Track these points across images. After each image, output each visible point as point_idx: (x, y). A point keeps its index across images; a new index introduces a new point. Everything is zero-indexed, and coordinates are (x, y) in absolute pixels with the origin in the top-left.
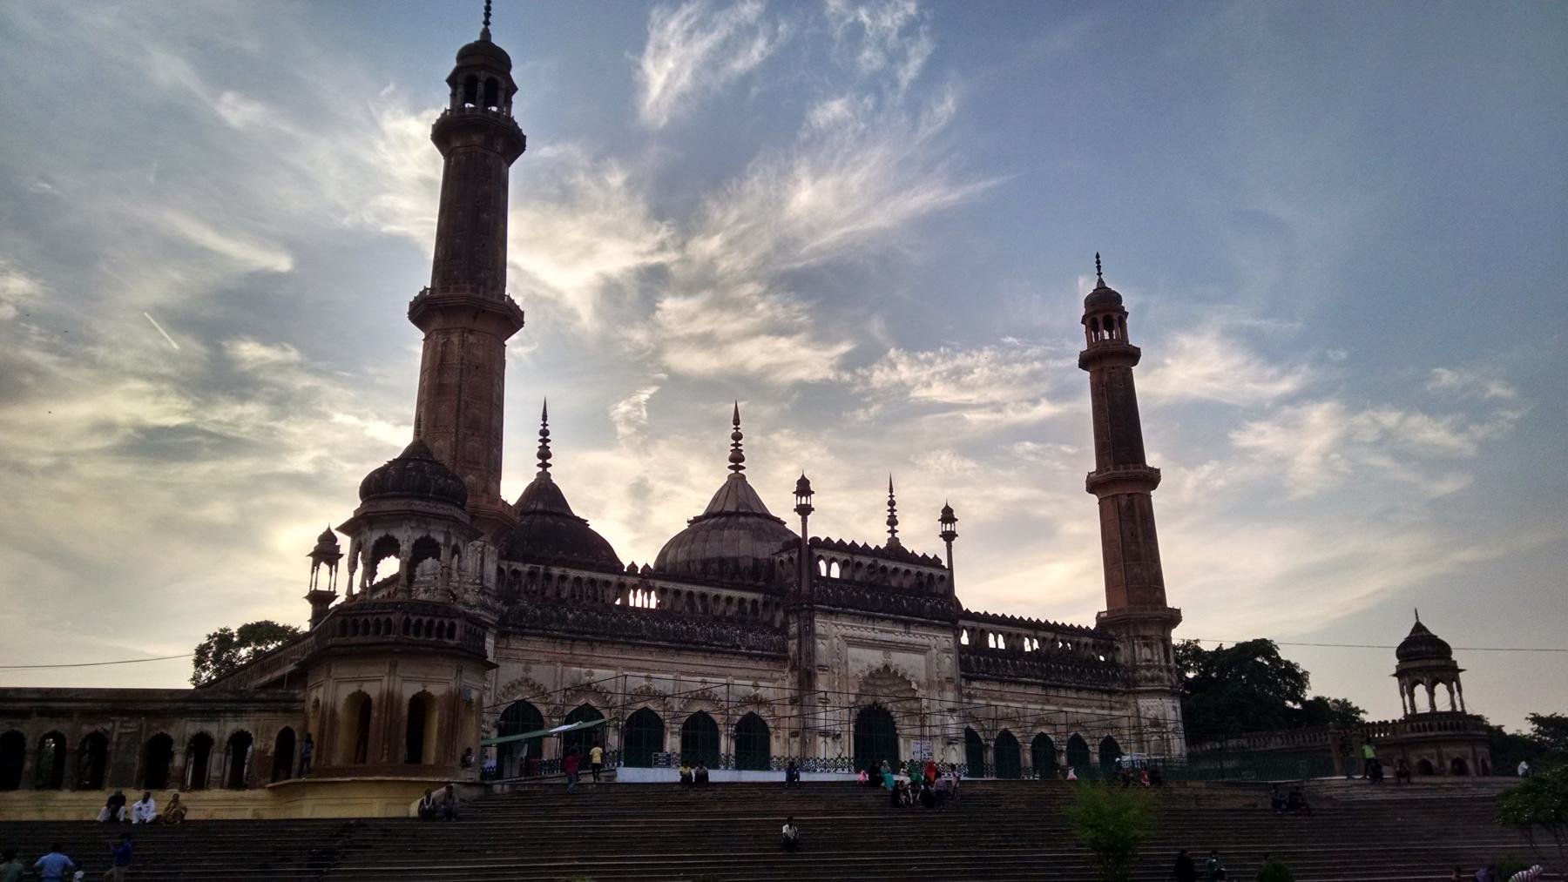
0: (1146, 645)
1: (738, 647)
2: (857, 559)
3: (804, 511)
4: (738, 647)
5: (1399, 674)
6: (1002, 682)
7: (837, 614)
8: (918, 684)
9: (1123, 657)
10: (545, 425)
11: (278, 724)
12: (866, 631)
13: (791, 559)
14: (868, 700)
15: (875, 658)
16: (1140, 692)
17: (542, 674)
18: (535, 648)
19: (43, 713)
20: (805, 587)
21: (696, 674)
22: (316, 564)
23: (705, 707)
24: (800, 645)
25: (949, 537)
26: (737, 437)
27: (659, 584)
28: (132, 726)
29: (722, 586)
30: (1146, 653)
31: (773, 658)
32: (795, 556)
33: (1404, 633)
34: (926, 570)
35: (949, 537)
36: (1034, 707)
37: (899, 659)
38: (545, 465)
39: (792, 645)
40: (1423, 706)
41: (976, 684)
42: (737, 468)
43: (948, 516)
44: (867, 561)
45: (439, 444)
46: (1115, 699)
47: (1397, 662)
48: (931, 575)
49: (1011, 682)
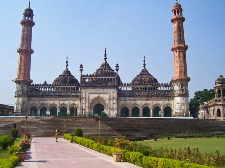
0: (177, 86)
2: (92, 77)
3: (81, 71)
4: (70, 95)
6: (134, 97)
7: (86, 88)
8: (106, 99)
12: (94, 91)
14: (97, 103)
15: (96, 96)
17: (36, 102)
18: (35, 98)
21: (62, 101)
23: (64, 106)
25: (117, 70)
26: (106, 54)
27: (56, 87)
29: (68, 85)
33: (218, 77)
36: (144, 102)
37: (101, 95)
38: (67, 67)
41: (126, 98)
42: (105, 60)
43: (117, 66)
46: (169, 98)
48: (111, 78)
49: (137, 97)
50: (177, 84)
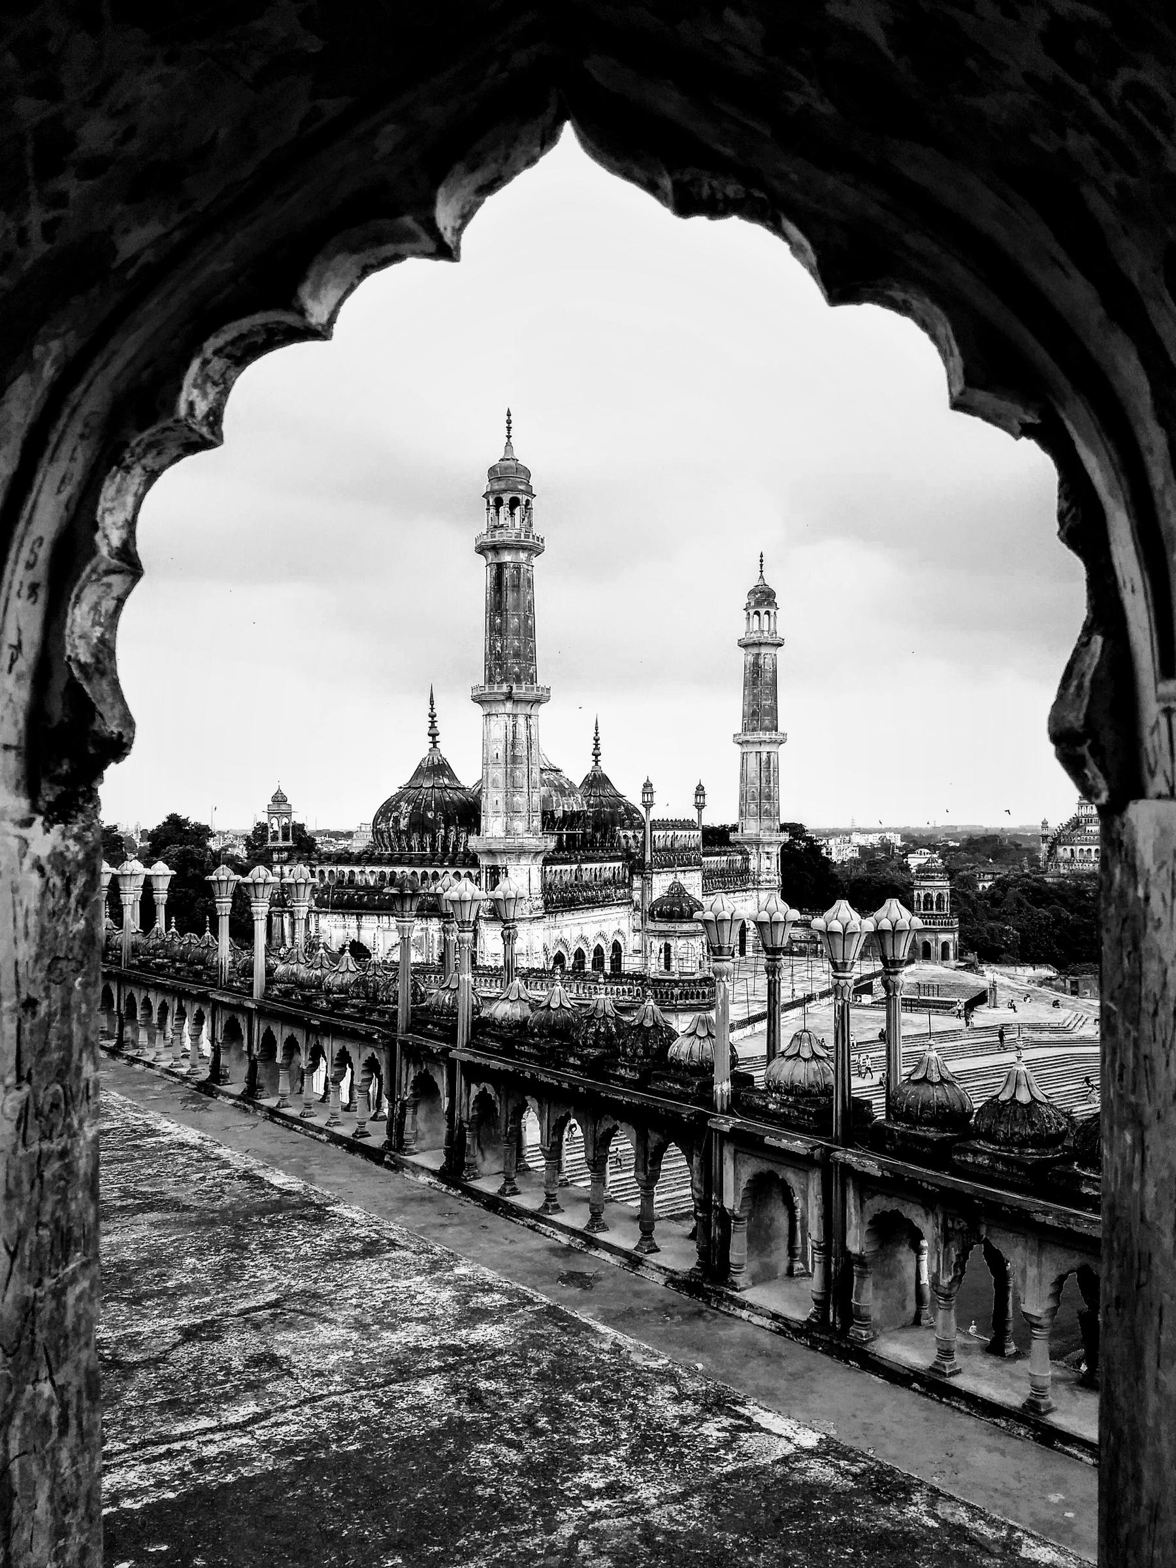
9: (753, 864)
10: (432, 709)
13: (635, 837)
20: (648, 858)
24: (643, 895)
25: (700, 807)
30: (765, 863)
31: (626, 904)
32: (640, 836)
35: (700, 807)
39: (636, 896)
43: (700, 791)
44: (670, 833)
45: (517, 798)
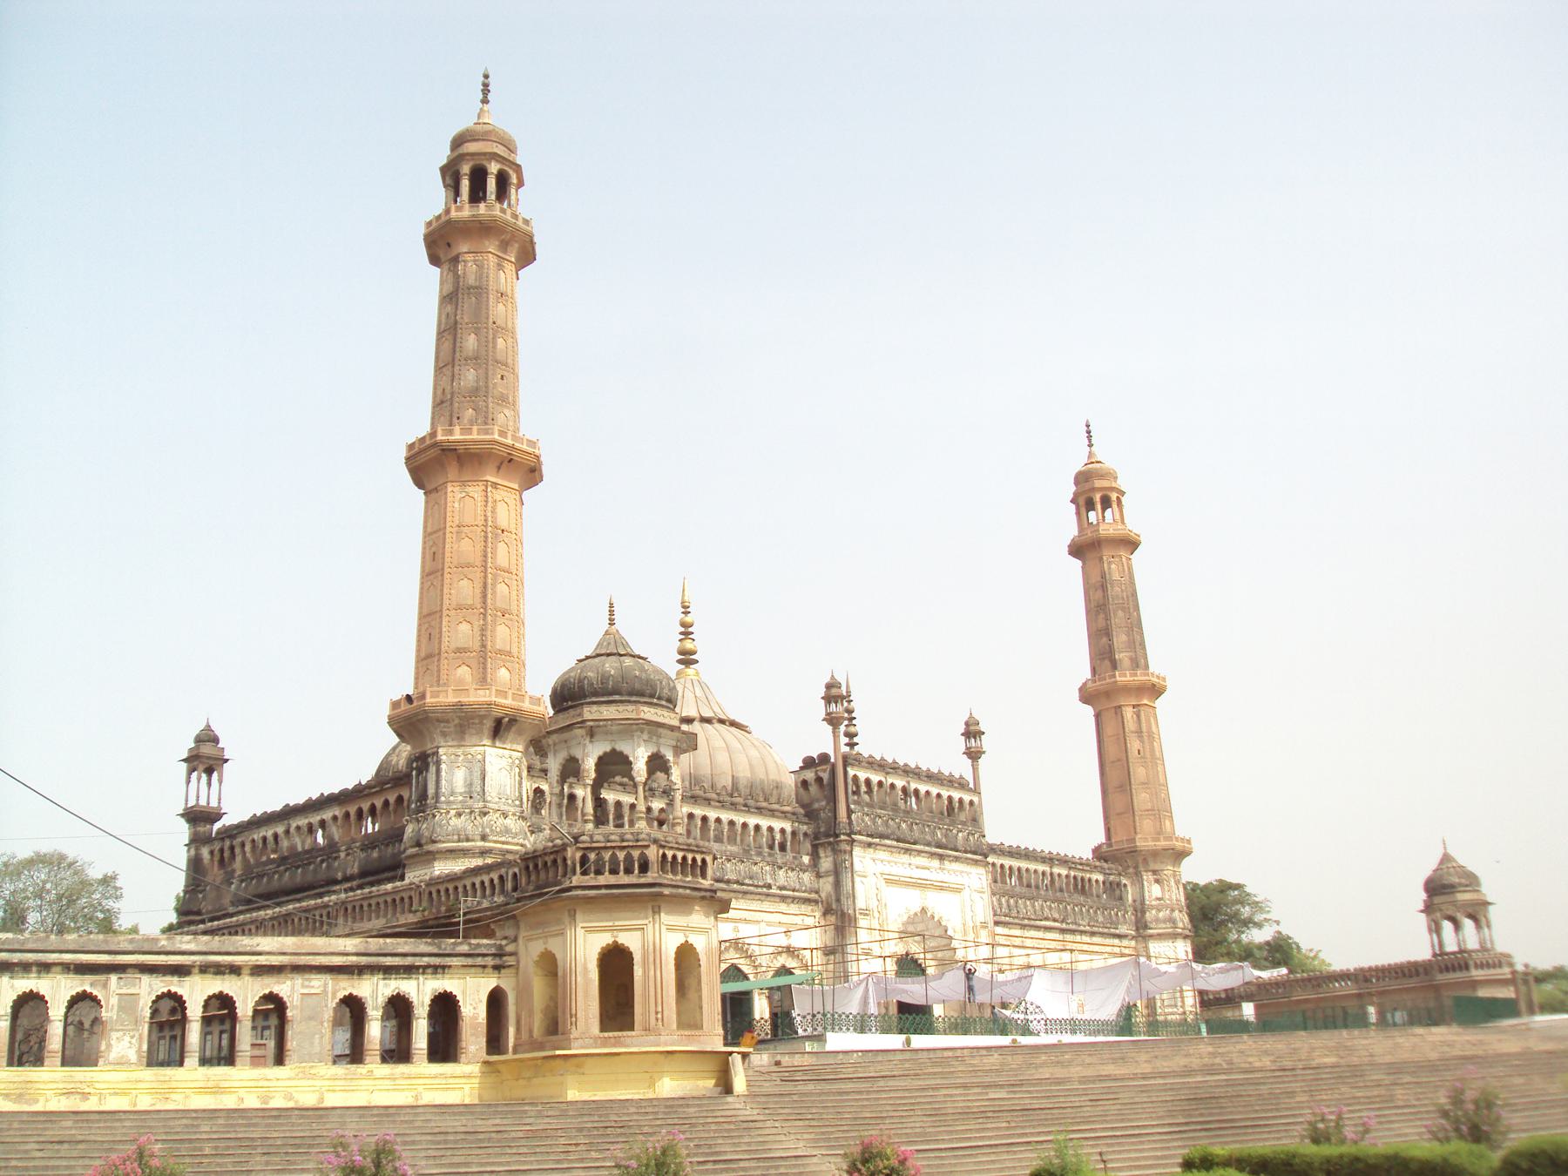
0: (1157, 881)
1: (769, 887)
4: (769, 887)
5: (1428, 909)
6: (1023, 927)
11: (489, 983)
13: (819, 780)
16: (1151, 936)
19: (204, 969)
22: (191, 771)
24: (837, 884)
25: (974, 755)
28: (317, 982)
32: (825, 776)
34: (956, 795)
35: (974, 755)
40: (1451, 946)
43: (972, 732)
47: (1424, 896)
50: (1155, 872)
